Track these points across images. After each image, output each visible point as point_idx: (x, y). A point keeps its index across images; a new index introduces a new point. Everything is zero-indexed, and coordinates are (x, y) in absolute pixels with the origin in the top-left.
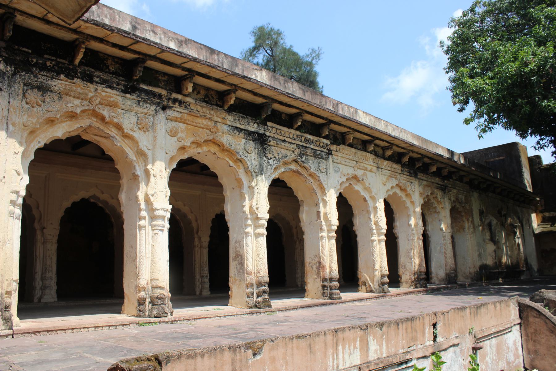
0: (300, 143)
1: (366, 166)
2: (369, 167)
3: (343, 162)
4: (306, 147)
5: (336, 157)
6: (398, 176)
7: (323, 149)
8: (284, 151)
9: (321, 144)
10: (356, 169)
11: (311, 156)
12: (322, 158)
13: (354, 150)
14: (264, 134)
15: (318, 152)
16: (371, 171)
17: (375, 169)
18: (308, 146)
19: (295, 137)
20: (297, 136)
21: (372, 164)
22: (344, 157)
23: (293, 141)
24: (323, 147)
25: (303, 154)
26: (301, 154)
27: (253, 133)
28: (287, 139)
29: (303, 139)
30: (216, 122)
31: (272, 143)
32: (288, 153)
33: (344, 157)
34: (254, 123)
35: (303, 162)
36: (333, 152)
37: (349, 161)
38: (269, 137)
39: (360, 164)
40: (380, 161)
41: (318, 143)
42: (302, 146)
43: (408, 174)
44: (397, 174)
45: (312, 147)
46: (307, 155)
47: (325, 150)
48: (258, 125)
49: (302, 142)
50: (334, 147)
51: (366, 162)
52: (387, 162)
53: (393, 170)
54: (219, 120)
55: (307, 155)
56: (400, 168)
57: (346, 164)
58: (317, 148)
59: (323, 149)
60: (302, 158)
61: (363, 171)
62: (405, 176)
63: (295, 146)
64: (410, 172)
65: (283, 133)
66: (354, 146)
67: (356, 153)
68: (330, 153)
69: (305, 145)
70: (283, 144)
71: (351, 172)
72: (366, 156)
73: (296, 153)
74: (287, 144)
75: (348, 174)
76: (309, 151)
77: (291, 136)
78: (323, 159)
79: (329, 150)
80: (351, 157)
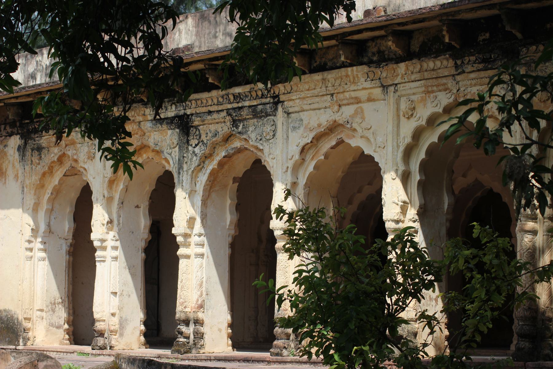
0: (229, 106)
1: (353, 94)
2: (363, 95)
3: (305, 107)
4: (240, 108)
5: (291, 103)
6: (450, 83)
7: (264, 101)
8: (213, 128)
9: (260, 93)
10: (336, 108)
11: (251, 119)
12: (267, 115)
13: (317, 77)
14: (185, 114)
15: (260, 107)
16: (370, 100)
17: (378, 91)
18: (240, 105)
19: (221, 100)
20: (223, 97)
21: (368, 84)
22: (304, 98)
23: (220, 108)
24: (263, 96)
25: (240, 121)
26: (235, 123)
27: (174, 118)
28: (211, 109)
29: (232, 98)
30: (140, 122)
31: (196, 121)
32: (218, 127)
33: (304, 98)
34: (171, 105)
35: (239, 133)
36: (282, 98)
37: (317, 99)
38: (192, 115)
39: (341, 96)
40: (384, 72)
41: (254, 94)
42: (234, 109)
43: (481, 66)
44: (444, 81)
45: (247, 103)
46: (245, 119)
47: (268, 100)
48: (176, 106)
49: (231, 103)
50: (280, 88)
51: (353, 87)
52: (402, 65)
53: (426, 75)
54: (141, 119)
55: (245, 119)
56: (451, 63)
57: (312, 106)
58: (255, 103)
59: (264, 101)
60: (237, 127)
61: (356, 106)
62: (473, 75)
63: (224, 114)
64: (484, 61)
65: (205, 101)
66: (329, 64)
67: (324, 79)
68: (277, 101)
69: (235, 105)
70: (209, 117)
71: (324, 118)
72: (347, 76)
73: (228, 124)
74: (215, 116)
75: (319, 125)
76: (245, 113)
77: (215, 101)
78: (270, 115)
79: (274, 97)
80: (316, 92)
